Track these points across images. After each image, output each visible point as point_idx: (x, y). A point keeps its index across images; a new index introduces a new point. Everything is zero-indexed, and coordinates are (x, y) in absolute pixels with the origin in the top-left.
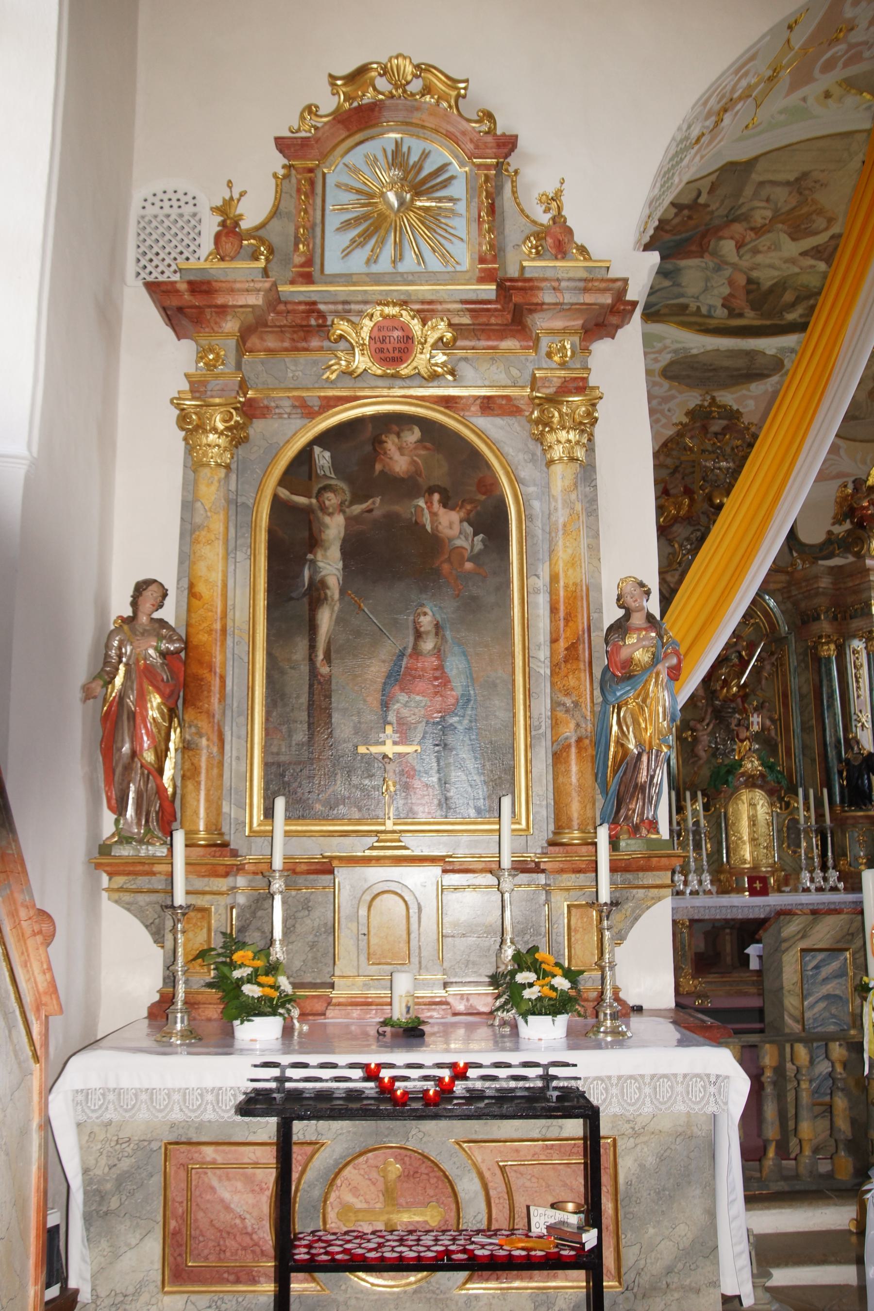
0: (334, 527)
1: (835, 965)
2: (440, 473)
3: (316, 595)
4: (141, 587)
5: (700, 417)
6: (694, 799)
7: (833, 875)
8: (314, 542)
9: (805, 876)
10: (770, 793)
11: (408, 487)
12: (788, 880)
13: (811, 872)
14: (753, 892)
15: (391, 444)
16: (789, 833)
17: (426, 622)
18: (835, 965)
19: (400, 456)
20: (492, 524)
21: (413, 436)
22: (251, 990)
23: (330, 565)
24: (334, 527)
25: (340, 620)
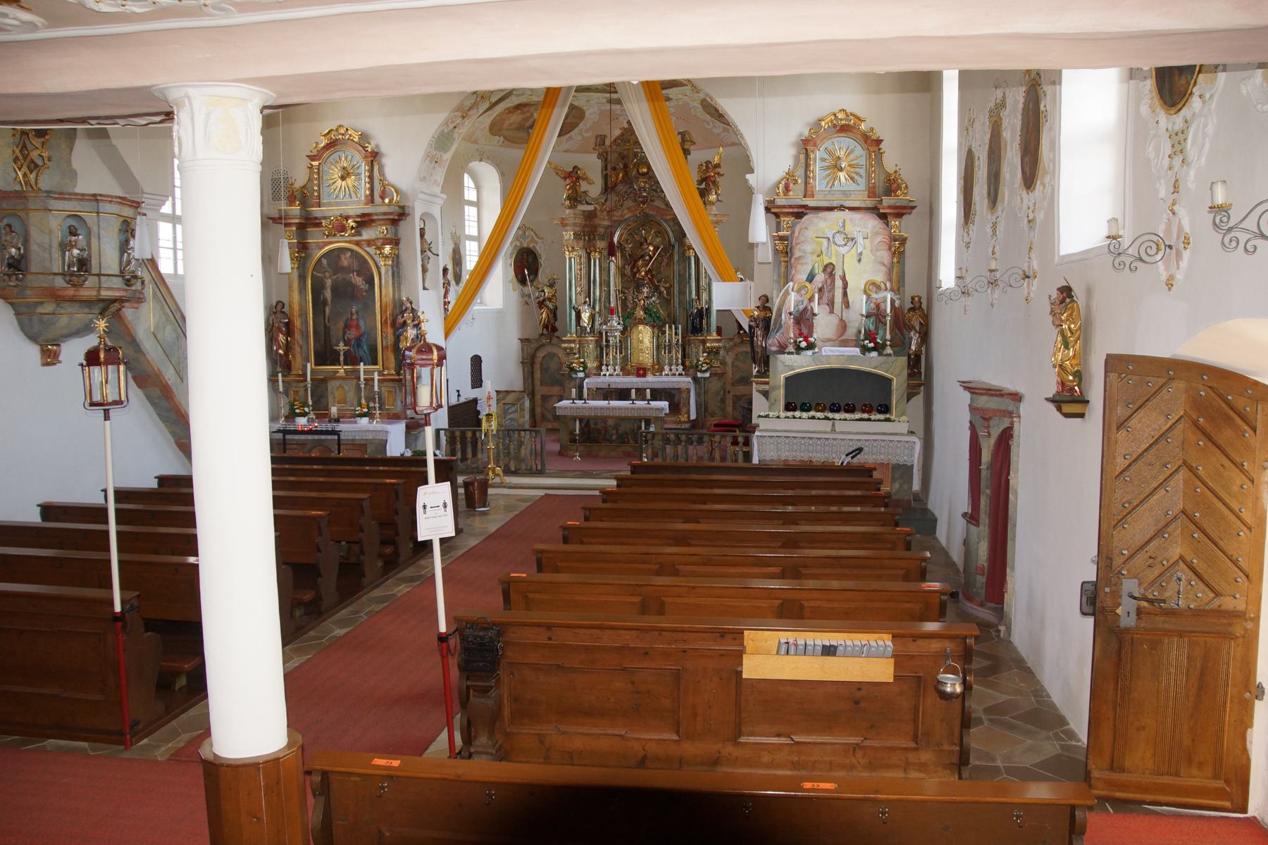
0: (329, 283)
3: (325, 303)
4: (278, 303)
7: (680, 368)
8: (323, 287)
9: (667, 368)
10: (653, 327)
11: (349, 270)
12: (658, 368)
13: (670, 365)
14: (639, 375)
15: (343, 257)
19: (345, 261)
20: (370, 282)
21: (349, 254)
23: (328, 294)
24: (329, 283)
25: (331, 311)
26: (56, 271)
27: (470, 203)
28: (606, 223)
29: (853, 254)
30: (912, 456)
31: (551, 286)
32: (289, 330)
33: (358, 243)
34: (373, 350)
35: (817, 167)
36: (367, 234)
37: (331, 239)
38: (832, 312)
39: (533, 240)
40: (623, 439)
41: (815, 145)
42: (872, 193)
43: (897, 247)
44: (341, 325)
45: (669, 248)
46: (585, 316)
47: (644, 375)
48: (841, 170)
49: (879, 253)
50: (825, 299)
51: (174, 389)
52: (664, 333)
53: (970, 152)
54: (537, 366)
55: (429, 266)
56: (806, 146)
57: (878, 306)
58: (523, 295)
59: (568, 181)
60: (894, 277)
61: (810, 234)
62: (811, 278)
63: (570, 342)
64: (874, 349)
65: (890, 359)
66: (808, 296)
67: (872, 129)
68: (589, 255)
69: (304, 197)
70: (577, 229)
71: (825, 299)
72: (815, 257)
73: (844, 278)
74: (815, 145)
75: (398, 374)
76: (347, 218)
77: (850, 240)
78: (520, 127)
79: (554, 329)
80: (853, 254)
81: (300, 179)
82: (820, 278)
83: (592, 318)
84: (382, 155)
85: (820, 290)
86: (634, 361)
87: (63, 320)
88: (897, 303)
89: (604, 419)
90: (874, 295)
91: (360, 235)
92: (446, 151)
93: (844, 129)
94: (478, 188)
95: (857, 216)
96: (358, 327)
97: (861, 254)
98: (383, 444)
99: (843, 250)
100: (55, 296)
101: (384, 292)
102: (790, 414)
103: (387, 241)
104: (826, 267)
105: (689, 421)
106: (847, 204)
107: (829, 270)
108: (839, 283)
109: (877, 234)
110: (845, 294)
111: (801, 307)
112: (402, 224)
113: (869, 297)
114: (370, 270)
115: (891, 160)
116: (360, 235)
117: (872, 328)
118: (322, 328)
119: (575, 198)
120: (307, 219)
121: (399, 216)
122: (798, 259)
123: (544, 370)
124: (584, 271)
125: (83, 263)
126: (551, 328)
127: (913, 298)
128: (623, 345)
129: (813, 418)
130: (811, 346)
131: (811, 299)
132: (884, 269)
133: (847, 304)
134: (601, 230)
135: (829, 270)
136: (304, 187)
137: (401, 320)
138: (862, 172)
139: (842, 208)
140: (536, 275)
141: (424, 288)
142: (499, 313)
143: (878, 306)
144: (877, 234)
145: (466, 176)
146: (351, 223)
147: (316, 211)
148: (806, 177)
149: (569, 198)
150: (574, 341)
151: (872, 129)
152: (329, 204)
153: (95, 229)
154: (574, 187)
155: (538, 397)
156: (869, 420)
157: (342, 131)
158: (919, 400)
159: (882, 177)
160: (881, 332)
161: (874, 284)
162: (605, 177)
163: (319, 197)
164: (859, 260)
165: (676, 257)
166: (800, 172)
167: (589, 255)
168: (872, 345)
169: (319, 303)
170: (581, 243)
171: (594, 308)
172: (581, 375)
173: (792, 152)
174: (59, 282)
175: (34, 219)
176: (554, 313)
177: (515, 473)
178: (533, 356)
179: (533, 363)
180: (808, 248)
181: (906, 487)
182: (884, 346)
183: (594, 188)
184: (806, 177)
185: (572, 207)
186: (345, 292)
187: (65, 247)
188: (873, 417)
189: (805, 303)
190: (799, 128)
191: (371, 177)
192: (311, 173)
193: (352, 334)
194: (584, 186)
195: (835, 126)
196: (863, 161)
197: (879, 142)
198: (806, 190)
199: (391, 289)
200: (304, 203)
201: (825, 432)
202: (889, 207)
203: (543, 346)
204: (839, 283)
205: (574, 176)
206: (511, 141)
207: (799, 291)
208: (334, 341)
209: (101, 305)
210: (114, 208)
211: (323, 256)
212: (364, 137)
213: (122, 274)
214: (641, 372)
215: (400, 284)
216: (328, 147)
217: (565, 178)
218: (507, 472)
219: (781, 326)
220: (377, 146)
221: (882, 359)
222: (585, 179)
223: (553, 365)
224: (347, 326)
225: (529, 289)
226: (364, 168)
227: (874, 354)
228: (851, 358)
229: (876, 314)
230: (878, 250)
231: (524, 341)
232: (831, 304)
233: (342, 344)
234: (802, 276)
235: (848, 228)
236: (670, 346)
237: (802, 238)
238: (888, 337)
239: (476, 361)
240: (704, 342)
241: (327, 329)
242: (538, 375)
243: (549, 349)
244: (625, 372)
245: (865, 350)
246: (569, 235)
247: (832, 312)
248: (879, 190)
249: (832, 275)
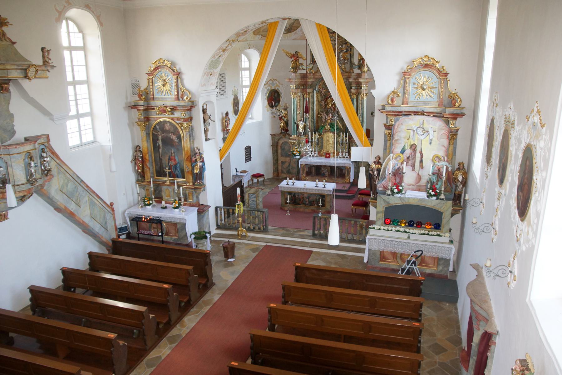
1: (254, 196)
2: (172, 130)
3: (159, 147)
6: (315, 133)
8: (158, 140)
9: (340, 154)
11: (168, 132)
13: (342, 152)
14: (326, 157)
17: (173, 152)
18: (254, 196)
19: (167, 127)
20: (179, 138)
21: (168, 124)
22: (146, 203)
23: (160, 143)
24: (160, 137)
27: (245, 69)
28: (312, 80)
29: (427, 141)
30: (450, 254)
31: (285, 110)
33: (172, 119)
34: (182, 171)
35: (410, 88)
36: (177, 114)
37: (160, 116)
38: (413, 170)
39: (277, 85)
40: (311, 204)
41: (410, 75)
42: (440, 104)
43: (453, 135)
44: (167, 158)
47: (329, 157)
48: (424, 89)
49: (442, 140)
50: (410, 163)
51: (76, 213)
52: (340, 136)
53: (492, 121)
54: (279, 147)
55: (209, 128)
56: (405, 75)
57: (439, 169)
58: (272, 113)
59: (293, 59)
60: (450, 152)
61: (404, 127)
62: (403, 152)
63: (293, 139)
64: (434, 195)
65: (443, 202)
66: (401, 161)
67: (443, 67)
68: (303, 95)
69: (146, 96)
70: (297, 83)
71: (410, 163)
72: (406, 140)
73: (421, 153)
74: (410, 75)
75: (194, 184)
76: (166, 107)
77: (426, 132)
79: (287, 130)
80: (427, 141)
81: (144, 85)
82: (408, 152)
83: (305, 127)
84: (182, 73)
85: (408, 158)
86: (325, 150)
88: (450, 169)
89: (302, 194)
90: (437, 163)
91: (174, 115)
92: (216, 68)
93: (427, 66)
94: (249, 61)
95: (431, 119)
96: (175, 160)
97: (431, 140)
99: (422, 137)
101: (186, 145)
102: (386, 228)
103: (186, 120)
104: (412, 146)
105: (350, 182)
106: (426, 110)
107: (413, 147)
108: (418, 155)
109: (441, 129)
110: (421, 161)
111: (397, 167)
112: (193, 109)
113: (434, 164)
114: (179, 132)
115: (454, 85)
116: (174, 115)
117: (435, 180)
118: (158, 159)
119: (296, 68)
120: (148, 106)
122: (396, 140)
123: (283, 149)
124: (301, 104)
126: (285, 130)
127: (459, 164)
129: (398, 231)
130: (400, 191)
131: (402, 163)
132: (444, 149)
133: (422, 166)
134: (310, 84)
135: (413, 147)
136: (146, 89)
137: (194, 159)
138: (436, 91)
139: (422, 113)
140: (279, 102)
141: (207, 139)
142: (260, 124)
143: (439, 169)
144: (441, 129)
145: (243, 56)
146: (168, 109)
147: (152, 102)
148: (404, 93)
149: (293, 68)
150: (295, 140)
151: (443, 67)
152: (159, 99)
155: (280, 162)
156: (428, 234)
157: (162, 61)
158: (458, 217)
159: (447, 95)
160: (439, 183)
161: (437, 157)
163: (153, 95)
164: (431, 143)
167: (303, 95)
168: (433, 193)
169: (156, 147)
170: (299, 90)
171: (305, 123)
172: (298, 157)
173: (397, 78)
176: (287, 123)
177: (253, 231)
178: (277, 143)
179: (277, 146)
180: (402, 135)
181: (445, 269)
182: (440, 194)
184: (404, 93)
185: (295, 72)
186: (167, 142)
188: (430, 233)
189: (399, 165)
190: (401, 65)
191: (177, 85)
192: (149, 82)
193: (172, 163)
194: (301, 61)
195: (421, 65)
196: (437, 85)
197: (446, 74)
198: (403, 101)
199: (189, 143)
200: (146, 99)
201: (404, 239)
202: (450, 114)
203: (282, 138)
204: (418, 155)
207: (396, 158)
208: (164, 166)
211: (157, 124)
212: (173, 64)
214: (328, 156)
215: (193, 140)
216: (157, 68)
217: (291, 58)
218: (249, 230)
219: (385, 177)
220: (180, 69)
221: (438, 201)
222: (301, 58)
223: (287, 148)
224: (170, 159)
225: (274, 110)
227: (435, 198)
228: (422, 200)
229: (438, 174)
230: (441, 138)
231: (273, 136)
232: (413, 166)
233: (167, 168)
234: (398, 150)
235: (425, 126)
236: (342, 144)
237: (399, 129)
238: (443, 189)
239: (248, 150)
241: (161, 160)
242: (279, 151)
244: (320, 155)
245: (429, 196)
246: (293, 86)
247: (413, 170)
248: (446, 102)
249: (414, 150)
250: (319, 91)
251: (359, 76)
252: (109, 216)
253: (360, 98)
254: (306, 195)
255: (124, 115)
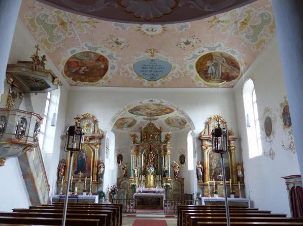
5: (149, 125)
16: (155, 181)
26: (13, 133)
28: (142, 148)
31: (126, 164)
32: (65, 167)
40: (153, 204)
45: (157, 155)
46: (136, 172)
78: (121, 124)
79: (126, 176)
83: (138, 172)
87: (11, 150)
98: (94, 200)
100: (13, 143)
103: (98, 144)
119: (134, 142)
121: (102, 137)
125: (23, 132)
128: (146, 182)
142: (113, 171)
146: (88, 138)
153: (28, 122)
154: (134, 139)
162: (141, 137)
165: (159, 157)
166: (207, 130)
173: (204, 125)
174: (14, 137)
175: (10, 117)
178: (120, 183)
183: (138, 140)
187: (18, 127)
190: (205, 119)
191: (94, 127)
197: (226, 123)
203: (123, 180)
205: (134, 136)
206: (118, 127)
209: (25, 147)
210: (35, 117)
212: (93, 117)
213: (34, 137)
226: (92, 125)
231: (118, 179)
240: (167, 179)
243: (125, 181)
246: (132, 151)
250: (145, 155)
251: (165, 146)
252: (47, 192)
253: (166, 158)
254: (149, 199)
255: (60, 141)
